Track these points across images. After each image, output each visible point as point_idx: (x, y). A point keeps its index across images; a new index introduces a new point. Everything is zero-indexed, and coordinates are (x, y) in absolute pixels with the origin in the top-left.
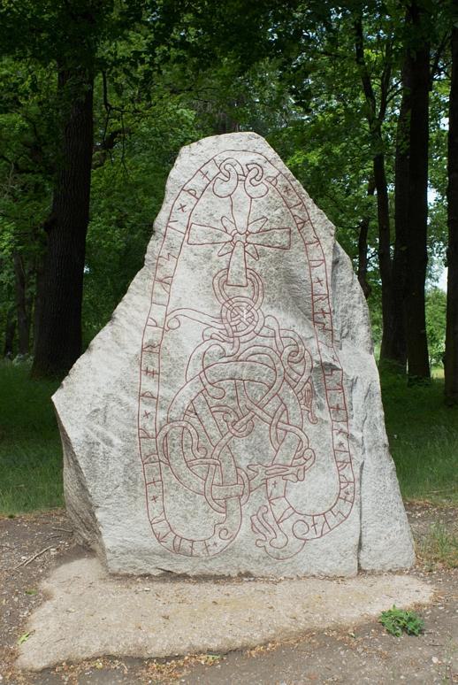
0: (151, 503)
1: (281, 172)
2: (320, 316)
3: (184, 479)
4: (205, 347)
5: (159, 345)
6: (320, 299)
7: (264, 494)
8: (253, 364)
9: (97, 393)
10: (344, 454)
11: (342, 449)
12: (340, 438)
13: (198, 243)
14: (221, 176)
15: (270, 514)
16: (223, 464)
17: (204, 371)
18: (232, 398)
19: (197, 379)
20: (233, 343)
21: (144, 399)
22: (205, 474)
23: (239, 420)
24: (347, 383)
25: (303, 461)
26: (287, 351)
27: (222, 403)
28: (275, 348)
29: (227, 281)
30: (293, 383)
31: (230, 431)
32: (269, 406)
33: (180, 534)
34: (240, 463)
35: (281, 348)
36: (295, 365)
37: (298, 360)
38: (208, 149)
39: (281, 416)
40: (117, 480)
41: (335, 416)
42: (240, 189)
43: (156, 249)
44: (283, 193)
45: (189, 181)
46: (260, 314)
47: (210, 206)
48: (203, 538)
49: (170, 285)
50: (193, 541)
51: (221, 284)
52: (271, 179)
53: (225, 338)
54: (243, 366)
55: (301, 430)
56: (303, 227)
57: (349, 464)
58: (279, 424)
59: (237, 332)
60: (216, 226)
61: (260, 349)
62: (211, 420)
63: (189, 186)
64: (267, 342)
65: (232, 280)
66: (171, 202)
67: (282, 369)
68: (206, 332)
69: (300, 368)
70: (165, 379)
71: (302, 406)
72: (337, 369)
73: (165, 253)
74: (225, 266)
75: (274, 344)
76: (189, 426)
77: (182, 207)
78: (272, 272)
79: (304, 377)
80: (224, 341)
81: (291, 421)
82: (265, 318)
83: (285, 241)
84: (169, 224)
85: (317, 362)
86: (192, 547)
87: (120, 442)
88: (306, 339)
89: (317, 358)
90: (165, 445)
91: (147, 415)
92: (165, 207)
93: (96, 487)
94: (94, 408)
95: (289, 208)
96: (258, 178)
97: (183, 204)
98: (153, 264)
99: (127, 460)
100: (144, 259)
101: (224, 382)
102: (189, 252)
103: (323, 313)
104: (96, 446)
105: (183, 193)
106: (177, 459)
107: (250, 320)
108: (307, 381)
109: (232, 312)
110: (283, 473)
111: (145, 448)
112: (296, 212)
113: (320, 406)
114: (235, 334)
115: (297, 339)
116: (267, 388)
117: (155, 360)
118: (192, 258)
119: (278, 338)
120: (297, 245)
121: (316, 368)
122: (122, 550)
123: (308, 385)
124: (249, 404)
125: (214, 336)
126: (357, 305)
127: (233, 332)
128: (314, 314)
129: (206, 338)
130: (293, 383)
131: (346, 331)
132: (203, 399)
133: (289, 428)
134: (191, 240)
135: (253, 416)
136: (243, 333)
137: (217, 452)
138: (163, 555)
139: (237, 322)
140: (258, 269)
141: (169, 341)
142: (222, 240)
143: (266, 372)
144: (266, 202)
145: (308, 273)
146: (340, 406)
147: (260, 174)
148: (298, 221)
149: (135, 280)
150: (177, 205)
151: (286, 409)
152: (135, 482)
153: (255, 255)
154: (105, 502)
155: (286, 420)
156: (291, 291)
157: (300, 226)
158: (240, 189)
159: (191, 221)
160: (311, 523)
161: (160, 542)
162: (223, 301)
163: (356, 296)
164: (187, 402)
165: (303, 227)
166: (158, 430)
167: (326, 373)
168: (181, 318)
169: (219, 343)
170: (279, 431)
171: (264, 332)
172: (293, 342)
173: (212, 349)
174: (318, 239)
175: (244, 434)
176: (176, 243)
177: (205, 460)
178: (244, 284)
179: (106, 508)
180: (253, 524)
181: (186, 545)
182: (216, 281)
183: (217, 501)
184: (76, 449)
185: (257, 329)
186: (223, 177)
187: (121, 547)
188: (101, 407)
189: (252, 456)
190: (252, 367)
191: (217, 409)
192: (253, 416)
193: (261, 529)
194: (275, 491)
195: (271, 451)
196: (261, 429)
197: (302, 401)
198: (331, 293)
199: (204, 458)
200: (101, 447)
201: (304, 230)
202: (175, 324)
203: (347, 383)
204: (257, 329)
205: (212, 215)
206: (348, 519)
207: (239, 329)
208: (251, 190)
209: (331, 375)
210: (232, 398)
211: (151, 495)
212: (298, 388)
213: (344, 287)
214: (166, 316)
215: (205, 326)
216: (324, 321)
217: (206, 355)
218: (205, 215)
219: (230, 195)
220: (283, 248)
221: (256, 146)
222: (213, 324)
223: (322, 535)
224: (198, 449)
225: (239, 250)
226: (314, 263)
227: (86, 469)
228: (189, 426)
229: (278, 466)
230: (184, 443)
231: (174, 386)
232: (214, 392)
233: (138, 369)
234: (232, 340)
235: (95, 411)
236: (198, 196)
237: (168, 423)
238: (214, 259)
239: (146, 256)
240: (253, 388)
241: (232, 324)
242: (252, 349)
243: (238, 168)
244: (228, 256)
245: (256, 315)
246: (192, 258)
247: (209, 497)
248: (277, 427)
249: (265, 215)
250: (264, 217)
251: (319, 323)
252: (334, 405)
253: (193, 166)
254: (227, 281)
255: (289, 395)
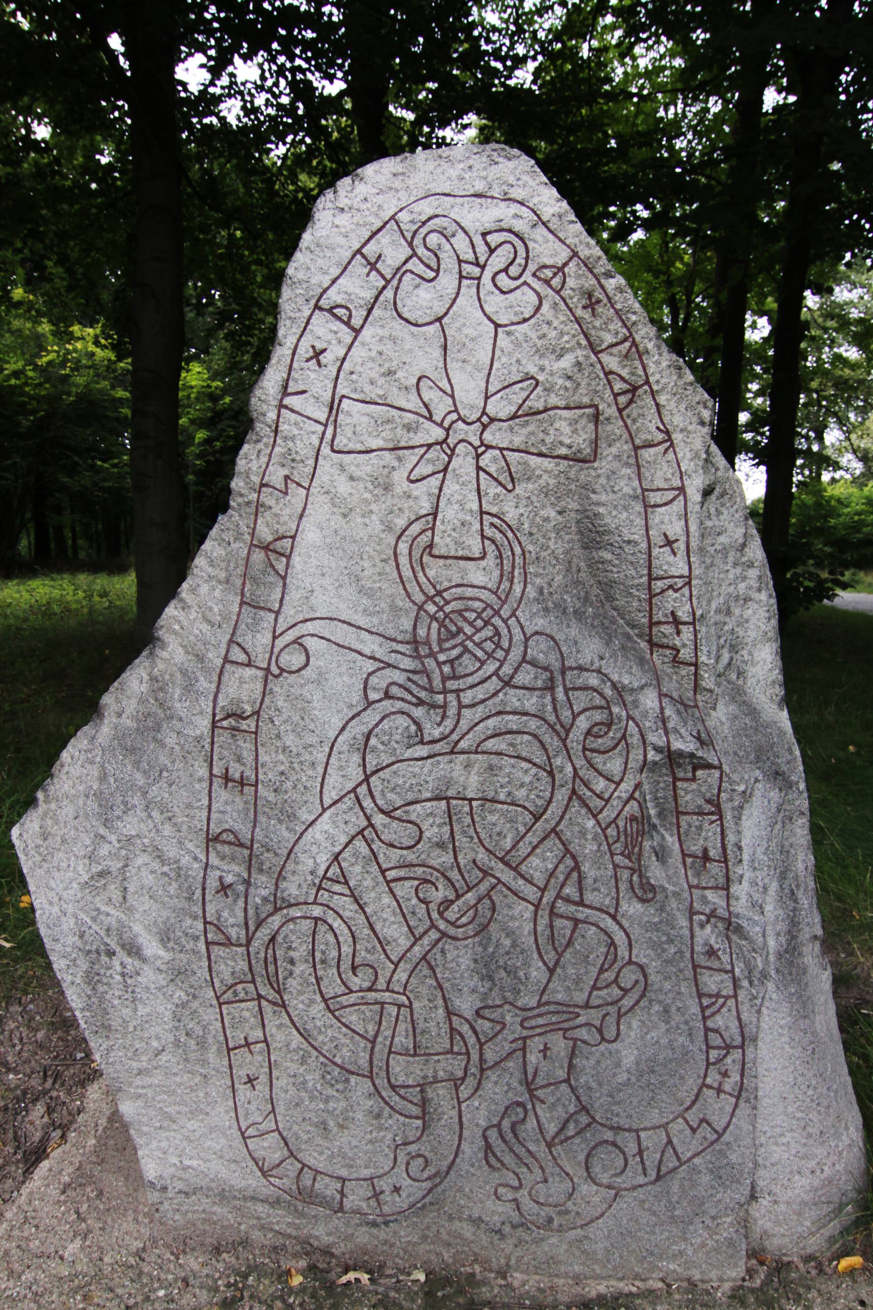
0: (244, 1092)
1: (575, 254)
2: (668, 629)
3: (321, 1038)
4: (371, 717)
5: (257, 713)
6: (671, 587)
7: (518, 1075)
8: (494, 760)
9: (102, 831)
10: (719, 977)
11: (716, 965)
12: (708, 935)
13: (359, 447)
14: (414, 265)
15: (531, 1123)
16: (416, 1005)
17: (367, 779)
18: (441, 845)
19: (349, 801)
20: (444, 706)
21: (219, 847)
22: (371, 1029)
23: (458, 897)
24: (731, 800)
25: (616, 992)
26: (583, 723)
27: (411, 856)
28: (552, 718)
29: (431, 546)
30: (596, 803)
31: (433, 926)
32: (535, 861)
33: (311, 1162)
34: (457, 1002)
35: (566, 714)
36: (598, 759)
37: (611, 743)
38: (381, 192)
39: (563, 885)
40: (158, 1038)
41: (698, 875)
42: (467, 300)
43: (254, 465)
44: (579, 312)
45: (334, 281)
46: (516, 630)
47: (388, 348)
48: (366, 1173)
49: (289, 558)
50: (344, 1180)
51: (416, 555)
52: (548, 273)
53: (423, 694)
54: (468, 766)
55: (614, 917)
56: (631, 401)
57: (731, 1003)
58: (560, 903)
59: (455, 677)
60: (403, 404)
61: (513, 723)
62: (387, 899)
63: (333, 296)
64: (531, 702)
65: (443, 544)
66: (290, 341)
67: (569, 769)
68: (373, 680)
69: (614, 766)
70: (271, 797)
71: (618, 859)
72: (709, 766)
73: (276, 476)
74: (426, 507)
75: (549, 708)
76: (330, 917)
77: (317, 354)
78: (547, 520)
79: (623, 786)
80: (420, 702)
81: (590, 897)
82: (527, 640)
83: (582, 440)
84: (288, 401)
85: (657, 749)
86: (342, 1193)
87: (161, 953)
88: (632, 690)
89: (656, 738)
90: (268, 962)
91: (224, 888)
92: (280, 354)
93: (109, 1050)
94: (96, 869)
95: (596, 353)
96: (514, 271)
97: (319, 346)
98: (248, 503)
99: (179, 993)
100: (228, 491)
101: (418, 807)
102: (335, 471)
103: (676, 622)
104: (104, 958)
105: (319, 318)
106: (300, 993)
107: (489, 646)
108: (631, 797)
109: (442, 624)
110: (565, 1025)
111: (223, 967)
112: (611, 362)
113: (661, 855)
114: (450, 685)
115: (608, 692)
116: (529, 818)
117: (246, 747)
118: (343, 487)
119: (560, 690)
120: (614, 450)
121: (655, 763)
122: (180, 1185)
123: (633, 805)
124: (482, 856)
125: (394, 690)
126: (756, 596)
127: (444, 679)
128: (651, 624)
129: (373, 696)
130: (596, 803)
131: (726, 656)
132: (364, 850)
133: (583, 913)
134: (341, 442)
135: (493, 887)
136: (470, 680)
137: (401, 975)
138: (276, 1203)
139: (455, 653)
140: (511, 516)
141: (280, 704)
142: (418, 439)
143: (527, 779)
144: (533, 335)
145: (639, 521)
146: (712, 853)
147: (520, 260)
148: (618, 386)
149: (207, 545)
150: (304, 350)
151: (577, 867)
152: (202, 1044)
153: (504, 478)
154: (138, 1081)
155: (576, 897)
156: (594, 565)
157: (623, 400)
158: (467, 300)
159: (341, 390)
160: (631, 1148)
161: (264, 1174)
162: (419, 598)
163: (753, 573)
164: (323, 860)
165: (631, 401)
166: (252, 928)
167: (681, 775)
168: (309, 642)
169: (405, 707)
170: (558, 923)
171: (525, 677)
172: (598, 701)
173: (385, 725)
174: (667, 433)
175: (470, 930)
176: (304, 448)
177: (371, 995)
178: (476, 552)
179: (140, 1096)
180: (488, 1147)
181: (327, 1188)
182: (403, 548)
183: (402, 1092)
184: (59, 964)
185: (507, 670)
186: (420, 269)
187: (180, 1179)
188: (115, 866)
189: (488, 985)
190: (491, 768)
191: (402, 873)
192: (493, 887)
193: (508, 1159)
194: (545, 1066)
195: (537, 972)
196: (513, 918)
197: (618, 847)
198: (696, 572)
199: (370, 989)
200: (116, 963)
201: (634, 410)
202: (294, 659)
203: (731, 800)
204: (507, 670)
205: (390, 373)
206: (726, 1137)
207: (460, 671)
208: (495, 303)
209: (694, 779)
210: (441, 845)
211: (243, 1073)
212: (607, 815)
213: (724, 552)
214: (275, 638)
215: (370, 666)
216: (678, 643)
217: (373, 741)
218: (374, 375)
219: (439, 320)
220: (577, 459)
221: (512, 180)
222: (393, 658)
223: (659, 1178)
224: (354, 968)
225: (463, 463)
226: (655, 498)
227: (83, 1010)
228: (330, 917)
229: (552, 1008)
230: (318, 955)
231: (292, 817)
232: (393, 831)
233: (203, 772)
234: (441, 697)
235: (101, 874)
236: (356, 322)
237: (277, 910)
238: (398, 490)
239: (233, 485)
240: (492, 818)
241: (442, 657)
242: (491, 723)
243: (461, 242)
244: (435, 481)
245: (504, 631)
246: (343, 487)
247: (381, 1082)
248: (552, 913)
249: (533, 370)
250: (528, 377)
251: (668, 647)
252: (695, 848)
253: (342, 241)
254: (431, 546)
255: (583, 833)
